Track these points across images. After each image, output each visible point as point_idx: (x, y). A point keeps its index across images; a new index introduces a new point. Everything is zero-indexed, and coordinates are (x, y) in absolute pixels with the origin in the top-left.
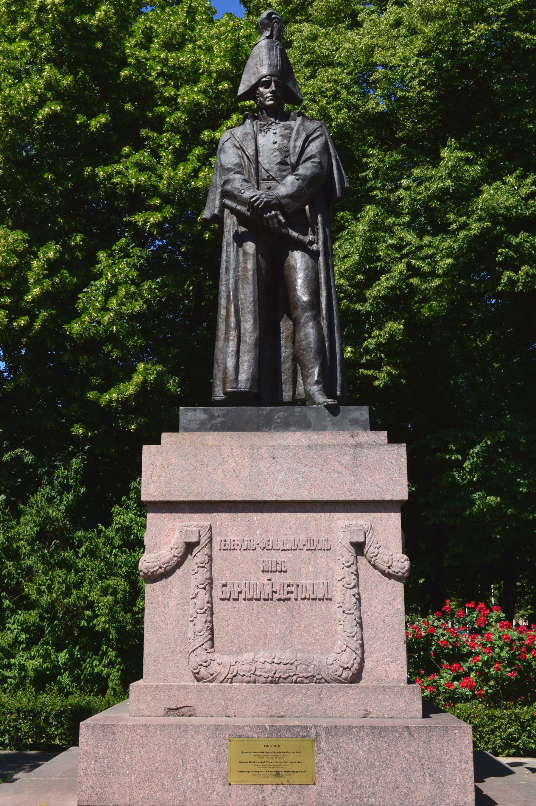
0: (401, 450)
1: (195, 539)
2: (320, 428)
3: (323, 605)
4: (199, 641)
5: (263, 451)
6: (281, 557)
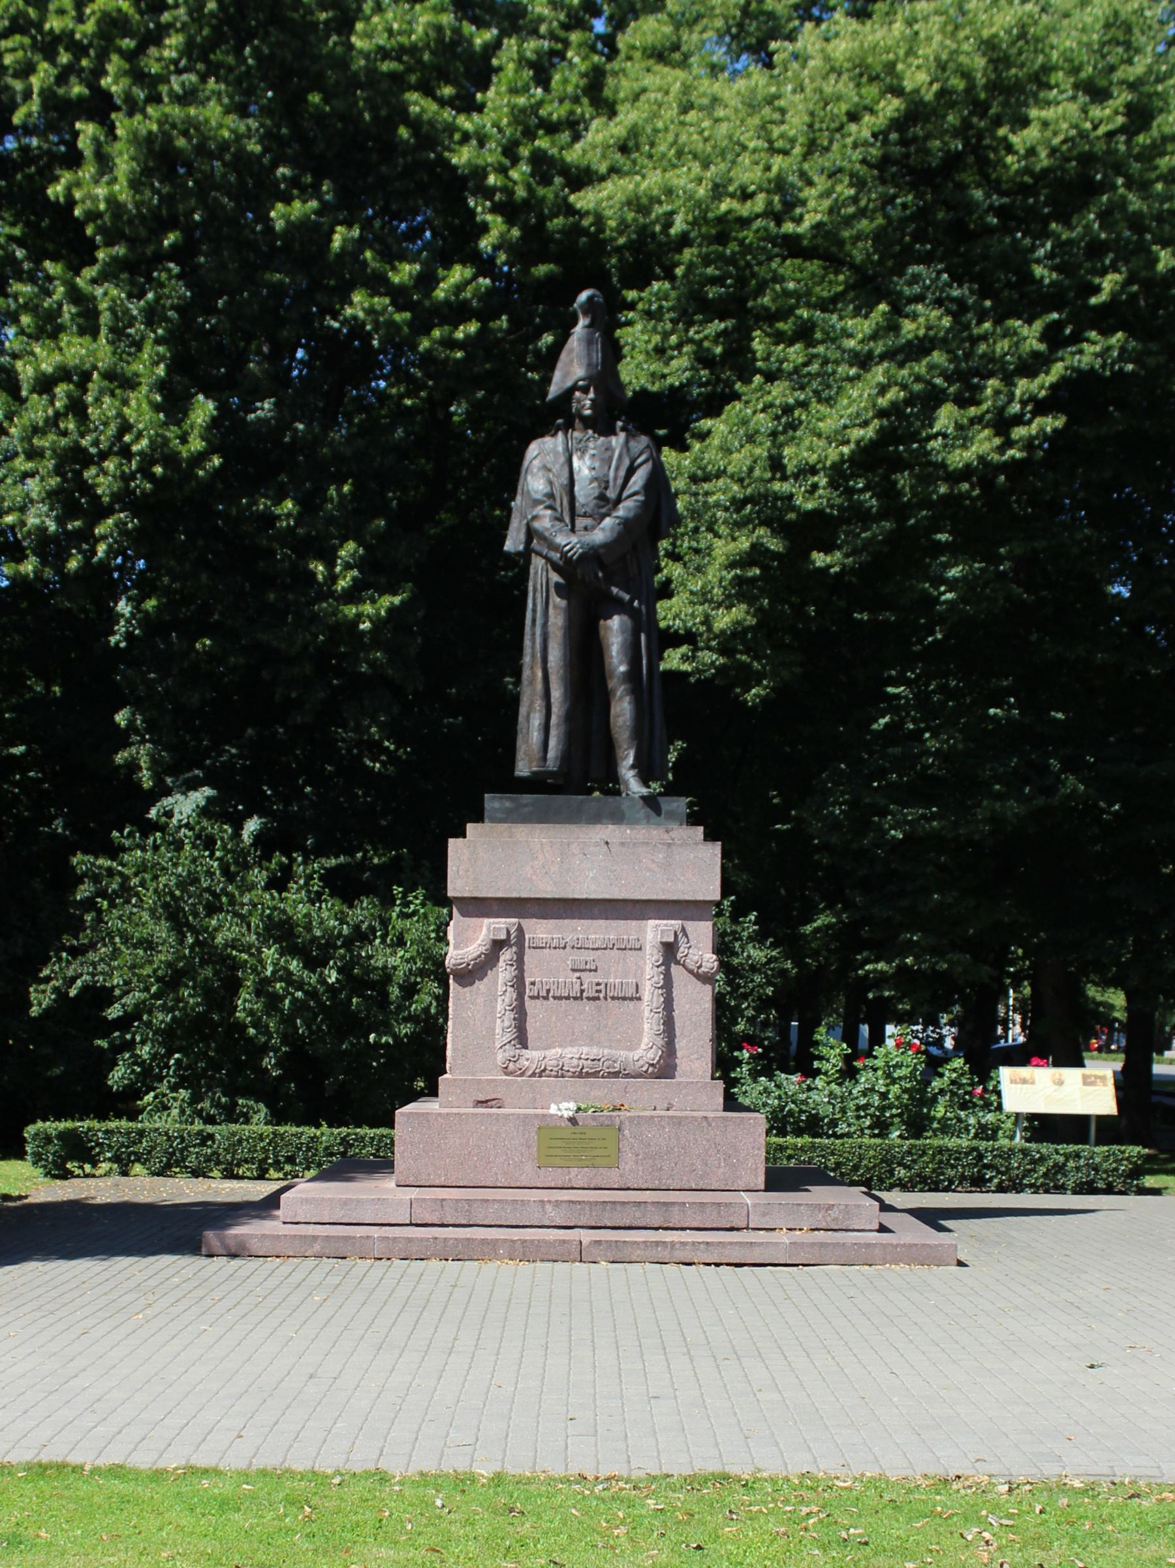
0: (716, 849)
1: (503, 936)
2: (633, 822)
3: (631, 1004)
4: (508, 1037)
5: (575, 848)
6: (589, 956)
